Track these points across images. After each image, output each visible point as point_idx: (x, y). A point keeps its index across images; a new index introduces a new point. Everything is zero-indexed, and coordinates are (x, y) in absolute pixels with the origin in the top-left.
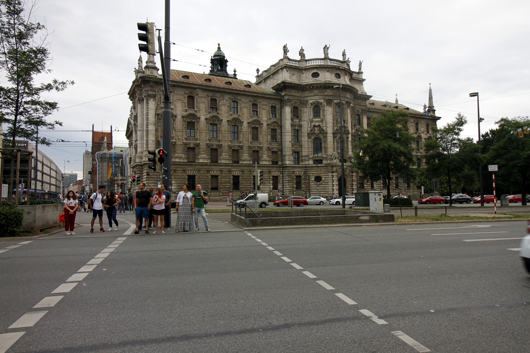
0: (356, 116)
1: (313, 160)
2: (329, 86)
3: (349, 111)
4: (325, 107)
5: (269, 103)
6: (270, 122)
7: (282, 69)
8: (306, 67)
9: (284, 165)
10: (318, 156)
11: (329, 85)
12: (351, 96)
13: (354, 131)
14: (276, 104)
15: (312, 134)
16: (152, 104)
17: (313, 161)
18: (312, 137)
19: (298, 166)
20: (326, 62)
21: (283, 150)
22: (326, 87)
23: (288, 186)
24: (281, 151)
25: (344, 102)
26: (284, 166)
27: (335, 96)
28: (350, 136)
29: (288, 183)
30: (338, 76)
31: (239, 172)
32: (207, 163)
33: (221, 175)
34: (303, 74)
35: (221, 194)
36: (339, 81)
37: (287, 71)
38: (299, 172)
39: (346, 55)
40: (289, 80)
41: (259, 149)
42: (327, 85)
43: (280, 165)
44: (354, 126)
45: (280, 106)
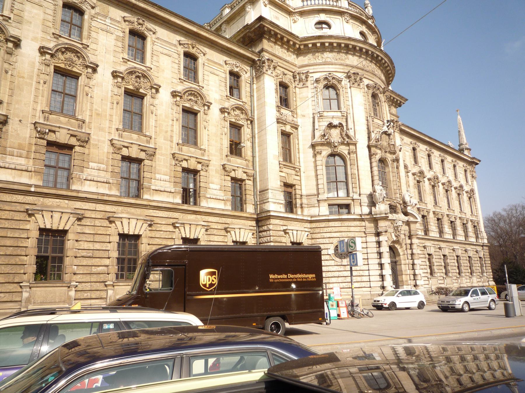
17: (327, 206)
31: (140, 223)
32: (30, 186)
33: (79, 229)
35: (72, 293)
41: (199, 167)
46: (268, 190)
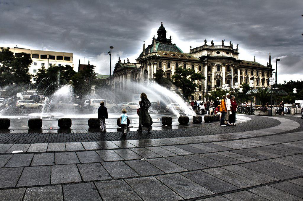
3: (232, 68)
13: (234, 77)
16: (155, 66)
24: (203, 85)
25: (230, 65)
28: (232, 79)
30: (228, 53)
44: (234, 74)
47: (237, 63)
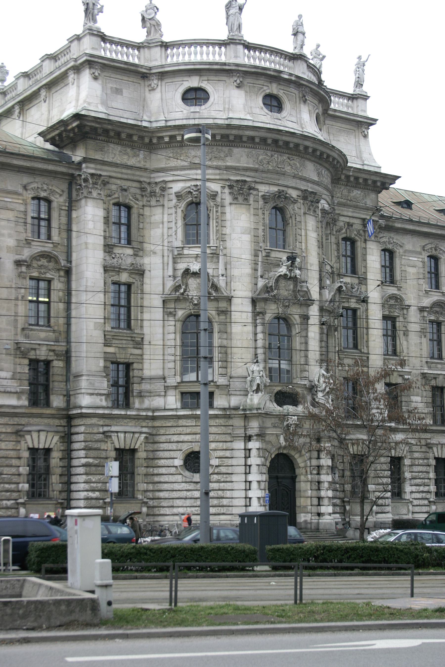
0: (342, 243)
1: (182, 393)
2: (241, 137)
4: (228, 209)
5: (25, 188)
6: (26, 254)
7: (77, 69)
8: (162, 66)
9: (76, 407)
10: (198, 381)
11: (241, 132)
12: (319, 174)
13: (328, 295)
14: (53, 192)
15: (177, 300)
17: (179, 397)
18: (180, 313)
19: (123, 412)
20: (233, 55)
21: (73, 354)
22: (231, 138)
23: (87, 486)
25: (294, 194)
26: (75, 412)
27: (263, 171)
29: (86, 474)
34: (153, 89)
36: (279, 122)
37: (96, 78)
38: (129, 436)
39: (304, 34)
40: (101, 108)
42: (234, 132)
43: (59, 409)
45: (65, 195)
46: (82, 375)
47: (357, 193)
